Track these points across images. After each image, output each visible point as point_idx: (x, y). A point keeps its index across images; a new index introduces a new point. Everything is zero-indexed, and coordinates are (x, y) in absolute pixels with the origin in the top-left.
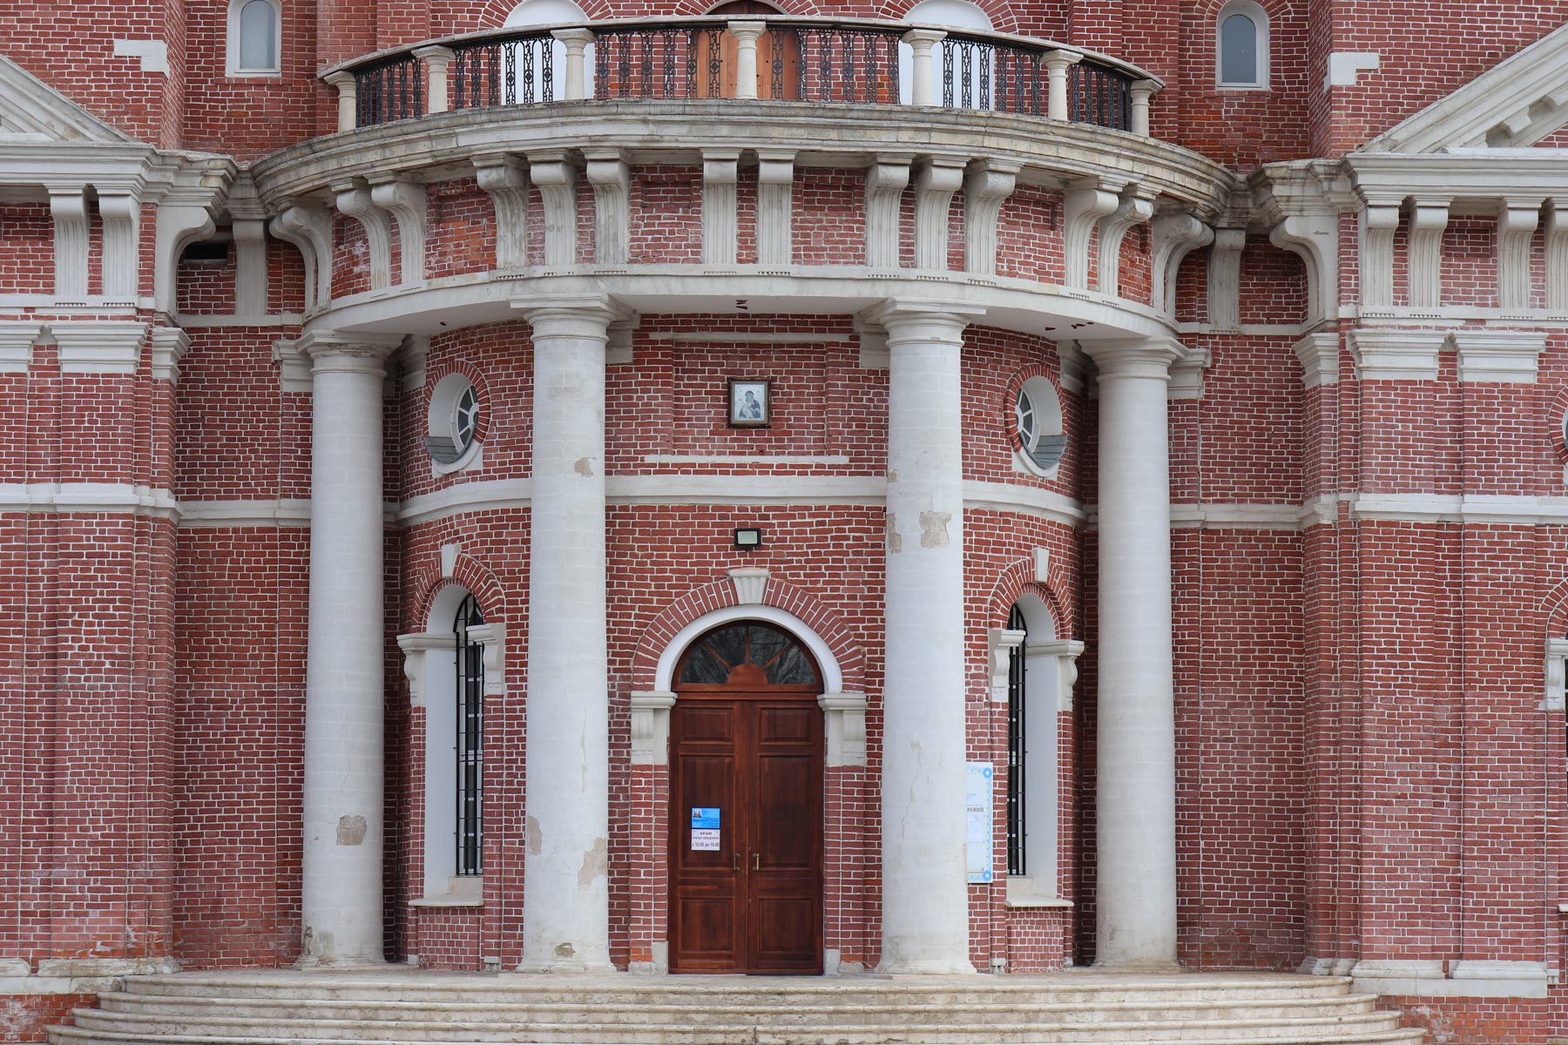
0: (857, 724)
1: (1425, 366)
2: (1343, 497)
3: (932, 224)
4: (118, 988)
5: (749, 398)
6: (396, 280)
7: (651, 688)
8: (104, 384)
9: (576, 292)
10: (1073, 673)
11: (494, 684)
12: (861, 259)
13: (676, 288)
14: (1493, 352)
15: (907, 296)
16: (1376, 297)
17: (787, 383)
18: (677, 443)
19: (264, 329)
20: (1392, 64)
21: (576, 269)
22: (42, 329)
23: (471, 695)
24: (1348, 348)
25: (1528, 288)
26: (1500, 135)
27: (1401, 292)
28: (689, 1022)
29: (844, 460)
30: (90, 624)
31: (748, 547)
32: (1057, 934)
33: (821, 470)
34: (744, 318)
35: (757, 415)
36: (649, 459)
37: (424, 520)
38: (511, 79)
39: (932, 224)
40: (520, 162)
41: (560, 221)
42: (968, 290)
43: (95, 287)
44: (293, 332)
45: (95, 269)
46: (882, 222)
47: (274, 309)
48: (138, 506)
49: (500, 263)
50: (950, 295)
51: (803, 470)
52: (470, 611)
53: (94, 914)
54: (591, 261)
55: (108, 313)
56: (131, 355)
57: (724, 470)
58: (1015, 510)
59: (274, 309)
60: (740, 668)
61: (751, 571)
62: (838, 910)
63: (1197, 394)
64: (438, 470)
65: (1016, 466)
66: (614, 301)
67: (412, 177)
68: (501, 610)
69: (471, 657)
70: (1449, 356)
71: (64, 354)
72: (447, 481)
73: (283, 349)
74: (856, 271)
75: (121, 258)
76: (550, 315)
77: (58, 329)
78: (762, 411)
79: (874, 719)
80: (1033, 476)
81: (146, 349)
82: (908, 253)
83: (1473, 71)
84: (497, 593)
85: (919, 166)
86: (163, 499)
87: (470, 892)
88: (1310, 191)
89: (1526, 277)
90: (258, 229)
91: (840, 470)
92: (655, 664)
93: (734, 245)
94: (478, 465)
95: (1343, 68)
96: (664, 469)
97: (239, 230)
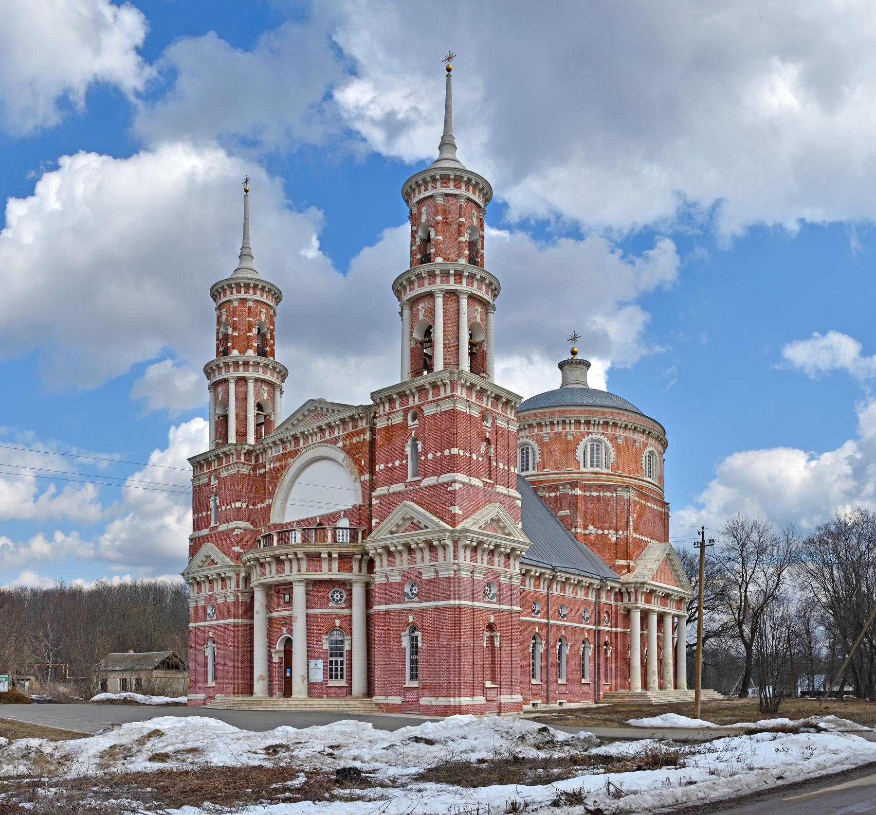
39: (295, 564)
74: (283, 575)
82: (291, 571)
96: (277, 611)
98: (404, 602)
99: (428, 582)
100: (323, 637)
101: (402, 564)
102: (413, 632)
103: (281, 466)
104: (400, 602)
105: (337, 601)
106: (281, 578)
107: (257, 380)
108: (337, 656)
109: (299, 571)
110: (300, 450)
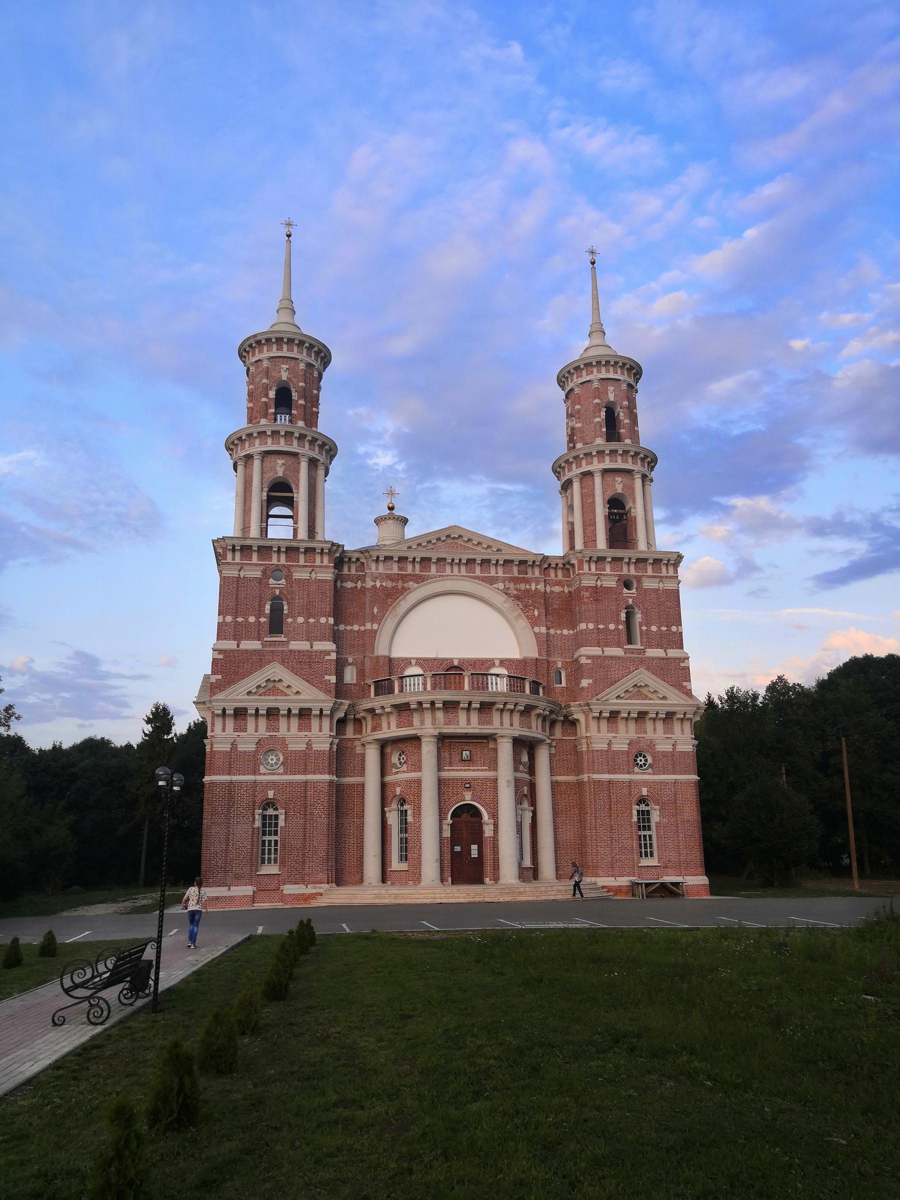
0: (492, 827)
1: (604, 746)
2: (589, 775)
3: (506, 716)
4: (326, 891)
6: (389, 728)
7: (447, 819)
8: (323, 752)
10: (531, 814)
11: (410, 819)
13: (454, 731)
14: (619, 744)
16: (593, 732)
17: (474, 751)
18: (451, 764)
19: (353, 739)
20: (595, 681)
21: (432, 727)
22: (309, 740)
23: (404, 822)
24: (589, 742)
25: (625, 729)
28: (470, 896)
29: (487, 768)
30: (319, 807)
31: (467, 788)
32: (531, 873)
33: (482, 770)
35: (468, 758)
36: (445, 768)
37: (388, 782)
38: (406, 686)
39: (506, 716)
40: (420, 704)
41: (428, 716)
42: (514, 731)
43: (321, 731)
44: (359, 739)
45: (321, 726)
46: (496, 716)
47: (355, 734)
48: (330, 780)
49: (414, 725)
50: (510, 732)
51: (478, 770)
52: (403, 802)
53: (321, 874)
54: (435, 725)
55: (324, 736)
56: (329, 746)
57: (462, 770)
58: (521, 778)
59: (355, 734)
60: (464, 814)
61: (468, 793)
62: (488, 868)
63: (553, 752)
64: (394, 770)
65: (521, 769)
66: (440, 733)
67: (394, 706)
68: (411, 802)
69: (404, 813)
70: (609, 744)
71: (313, 746)
72: (397, 773)
73: (357, 743)
75: (326, 723)
77: (313, 740)
78: (469, 757)
79: (496, 825)
80: (524, 771)
81: (331, 744)
83: (612, 684)
84: (411, 798)
86: (335, 778)
87: (404, 866)
88: (580, 709)
89: (624, 727)
90: (352, 717)
91: (486, 770)
92: (448, 814)
93: (466, 721)
94: (405, 769)
96: (448, 770)
97: (348, 717)
98: (633, 773)
99: (665, 754)
101: (627, 732)
102: (402, 805)
104: (629, 773)
105: (641, 766)
106: (486, 730)
108: (270, 834)
109: (511, 725)
110: (429, 577)
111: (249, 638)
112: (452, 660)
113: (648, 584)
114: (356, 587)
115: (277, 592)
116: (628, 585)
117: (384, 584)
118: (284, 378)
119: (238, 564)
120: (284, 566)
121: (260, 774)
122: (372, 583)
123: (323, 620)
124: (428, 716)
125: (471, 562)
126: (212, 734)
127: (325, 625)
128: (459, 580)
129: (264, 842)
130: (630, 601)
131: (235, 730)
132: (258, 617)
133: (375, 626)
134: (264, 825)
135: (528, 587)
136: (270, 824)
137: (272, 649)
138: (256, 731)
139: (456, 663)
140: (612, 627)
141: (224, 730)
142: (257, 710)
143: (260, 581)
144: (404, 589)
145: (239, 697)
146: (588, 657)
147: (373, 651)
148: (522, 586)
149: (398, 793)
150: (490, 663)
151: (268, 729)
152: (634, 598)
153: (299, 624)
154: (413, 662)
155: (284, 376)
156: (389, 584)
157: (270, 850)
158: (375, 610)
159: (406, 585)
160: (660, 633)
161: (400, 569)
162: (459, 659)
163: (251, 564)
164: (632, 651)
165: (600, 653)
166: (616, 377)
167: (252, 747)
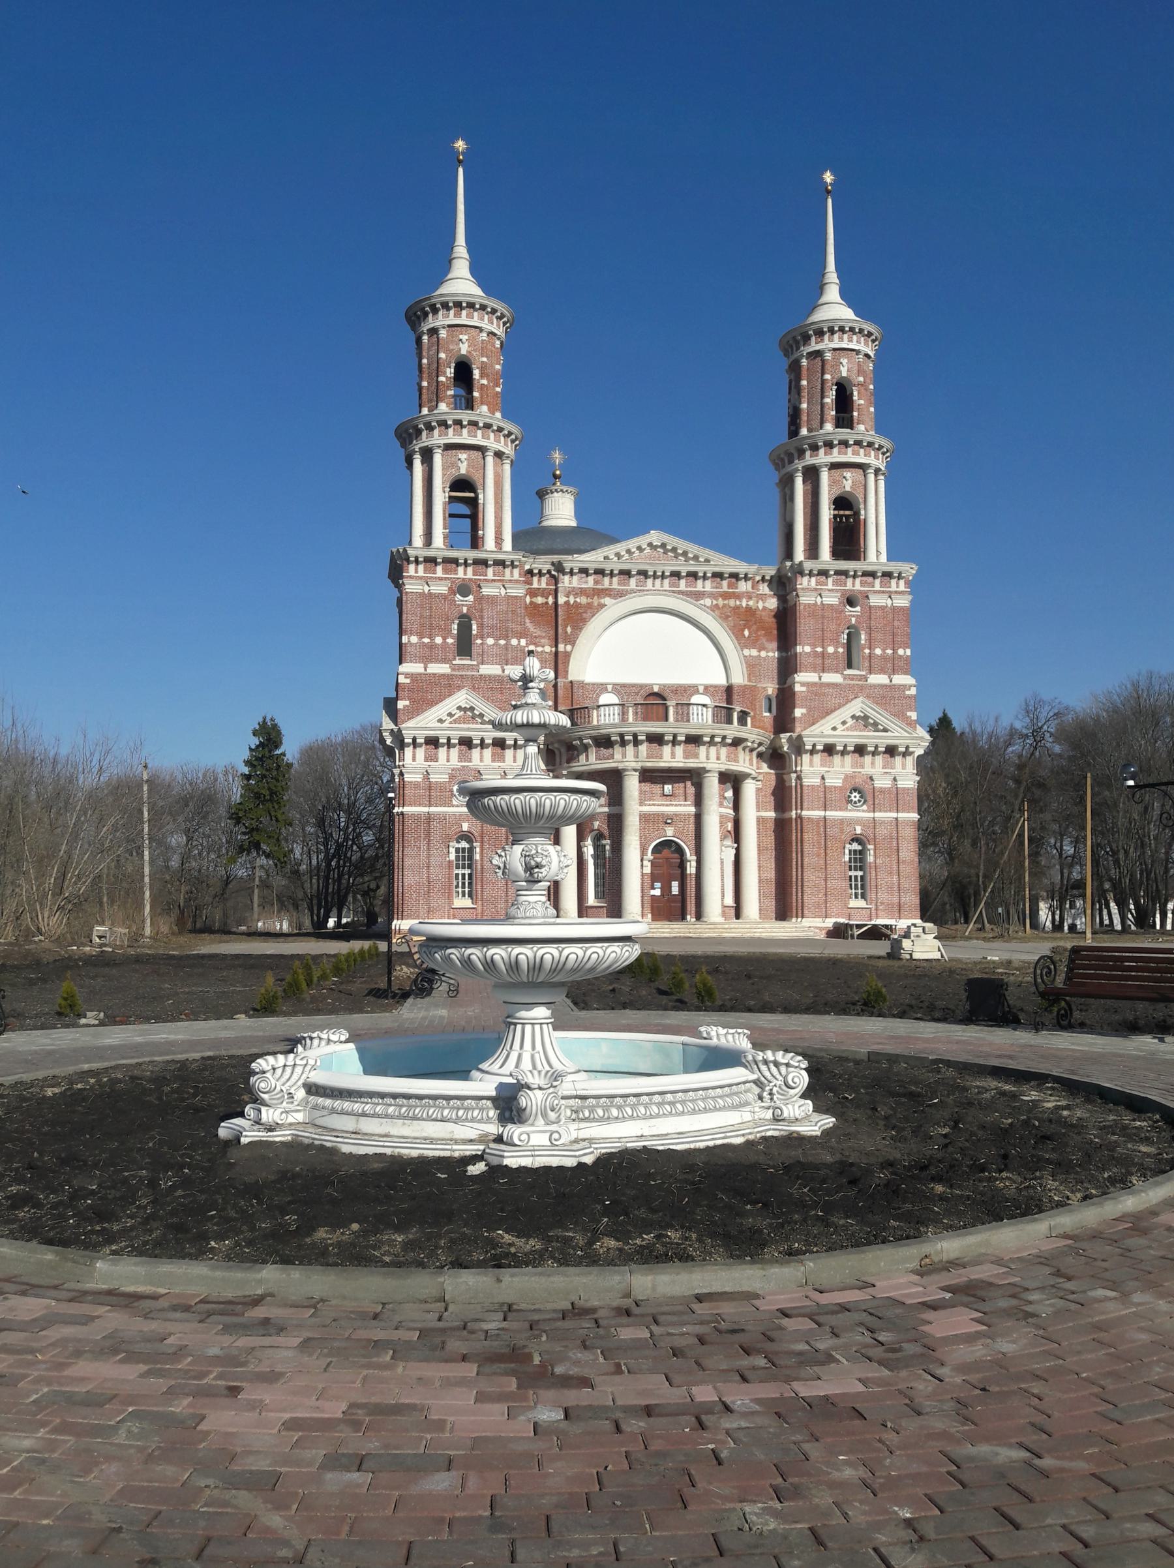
1: (817, 781)
5: (668, 788)
9: (634, 765)
10: (734, 851)
12: (698, 758)
14: (832, 778)
15: (708, 766)
20: (809, 711)
26: (834, 729)
27: (811, 765)
33: (685, 805)
34: (670, 770)
40: (622, 736)
41: (630, 749)
45: (515, 757)
50: (717, 766)
57: (663, 805)
74: (697, 761)
76: (627, 770)
83: (828, 714)
85: (713, 737)
95: (798, 712)
96: (650, 805)
98: (846, 809)
99: (883, 791)
100: (451, 844)
101: (843, 766)
103: (589, 605)
105: (855, 803)
106: (692, 764)
107: (449, 447)
109: (718, 758)
110: (627, 593)
111: (437, 661)
112: (651, 685)
113: (876, 601)
114: (547, 603)
115: (465, 610)
116: (851, 602)
117: (578, 600)
118: (464, 352)
119: (421, 578)
120: (470, 580)
121: (453, 806)
122: (565, 599)
123: (514, 642)
124: (630, 749)
125: (676, 574)
126: (401, 763)
127: (516, 647)
128: (660, 595)
129: (457, 875)
130: (853, 620)
131: (426, 760)
132: (444, 639)
133: (569, 648)
134: (457, 858)
135: (738, 603)
136: (464, 859)
137: (461, 673)
138: (448, 761)
139: (656, 689)
140: (831, 650)
141: (414, 760)
142: (449, 739)
143: (445, 597)
144: (602, 606)
145: (429, 725)
146: (803, 684)
147: (566, 676)
148: (732, 603)
149: (596, 827)
150: (692, 690)
151: (460, 759)
152: (857, 617)
153: (489, 646)
154: (610, 688)
155: (464, 349)
156: (583, 600)
157: (463, 884)
158: (569, 629)
159: (602, 601)
160: (884, 657)
161: (596, 582)
162: (660, 685)
163: (436, 578)
164: (851, 678)
165: (816, 680)
166: (851, 346)
167: (445, 778)
